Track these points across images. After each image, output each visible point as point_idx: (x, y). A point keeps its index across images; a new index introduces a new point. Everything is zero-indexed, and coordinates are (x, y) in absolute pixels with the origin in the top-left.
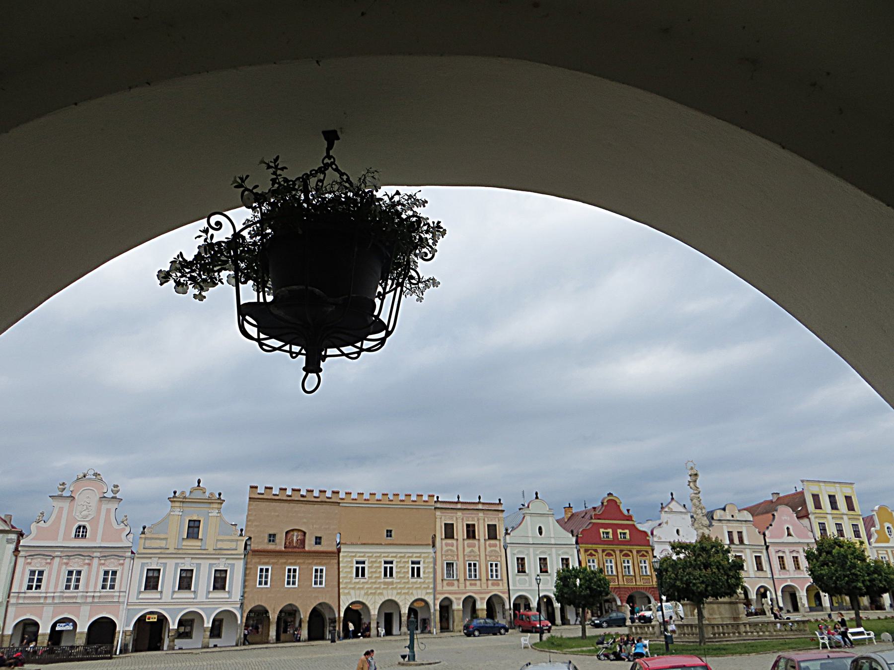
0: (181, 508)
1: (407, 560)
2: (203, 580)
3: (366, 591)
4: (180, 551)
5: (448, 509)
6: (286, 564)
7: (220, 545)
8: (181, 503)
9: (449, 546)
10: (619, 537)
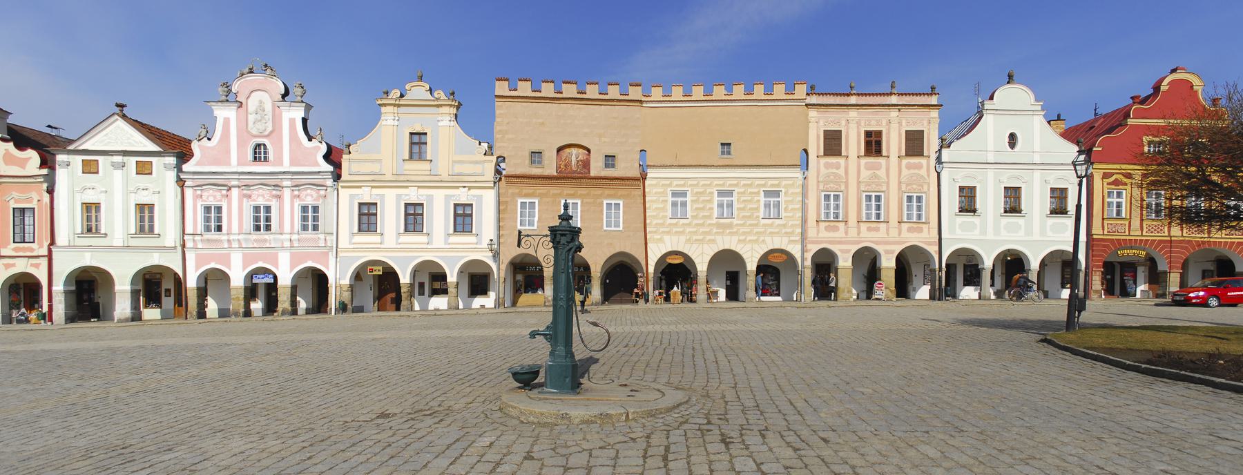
1: (756, 190)
2: (439, 217)
3: (688, 237)
4: (402, 178)
6: (560, 195)
7: (458, 169)
8: (396, 108)
9: (832, 168)
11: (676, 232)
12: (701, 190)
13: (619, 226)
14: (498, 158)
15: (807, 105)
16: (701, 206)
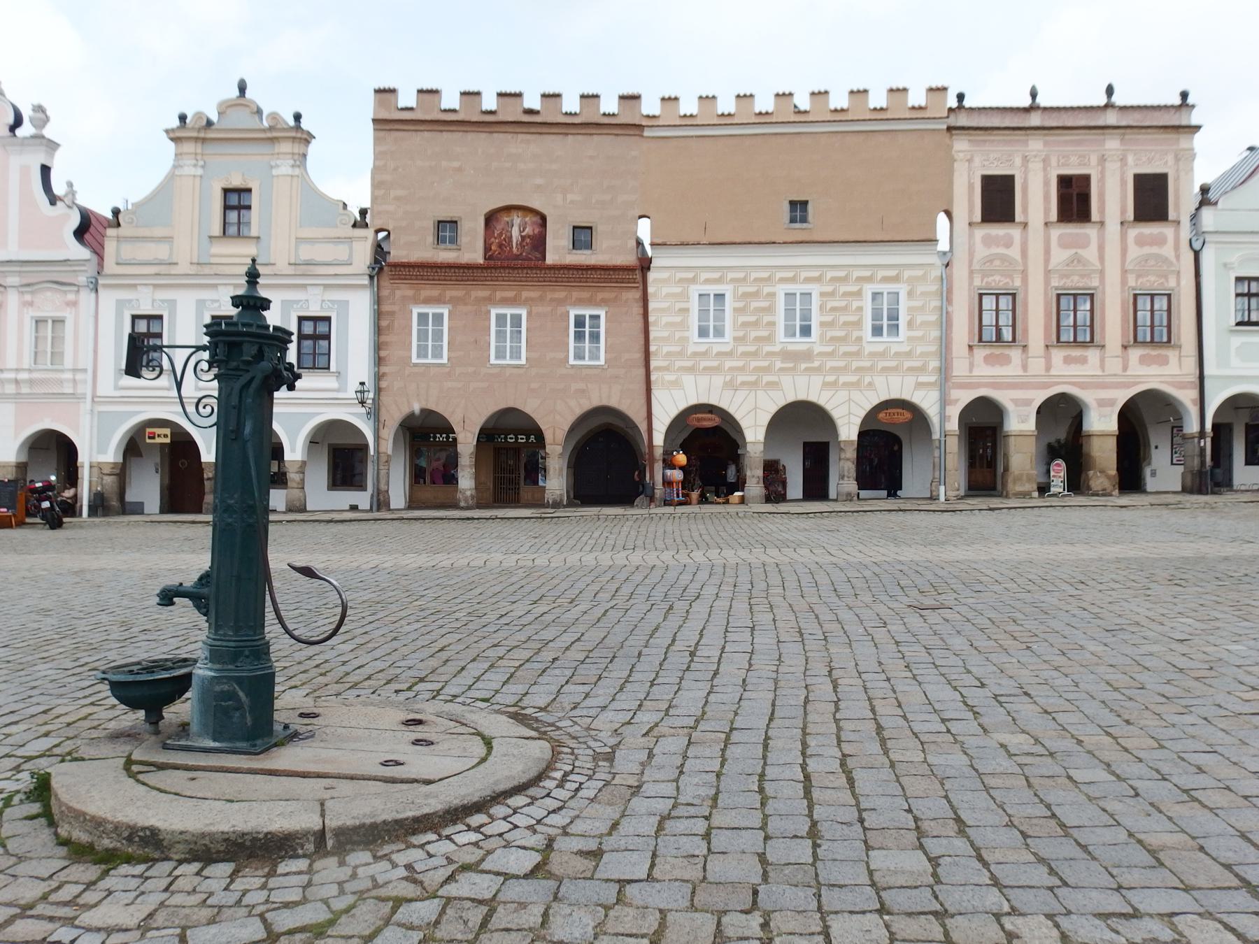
0: (199, 157)
1: (855, 289)
3: (728, 378)
4: (207, 270)
6: (491, 301)
7: (306, 253)
8: (199, 145)
11: (705, 369)
12: (752, 289)
13: (598, 358)
15: (949, 129)
16: (753, 319)
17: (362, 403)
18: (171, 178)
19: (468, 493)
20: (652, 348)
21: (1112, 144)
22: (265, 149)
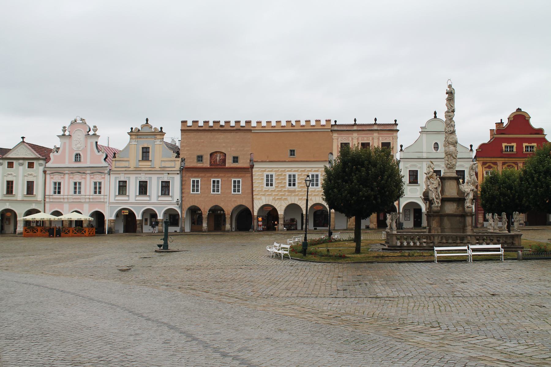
2: (154, 188)
3: (274, 197)
5: (344, 130)
6: (211, 177)
7: (164, 164)
10: (524, 151)
11: (268, 195)
14: (182, 159)
17: (178, 204)
18: (129, 144)
19: (205, 228)
20: (254, 189)
21: (376, 135)
22: (153, 137)
